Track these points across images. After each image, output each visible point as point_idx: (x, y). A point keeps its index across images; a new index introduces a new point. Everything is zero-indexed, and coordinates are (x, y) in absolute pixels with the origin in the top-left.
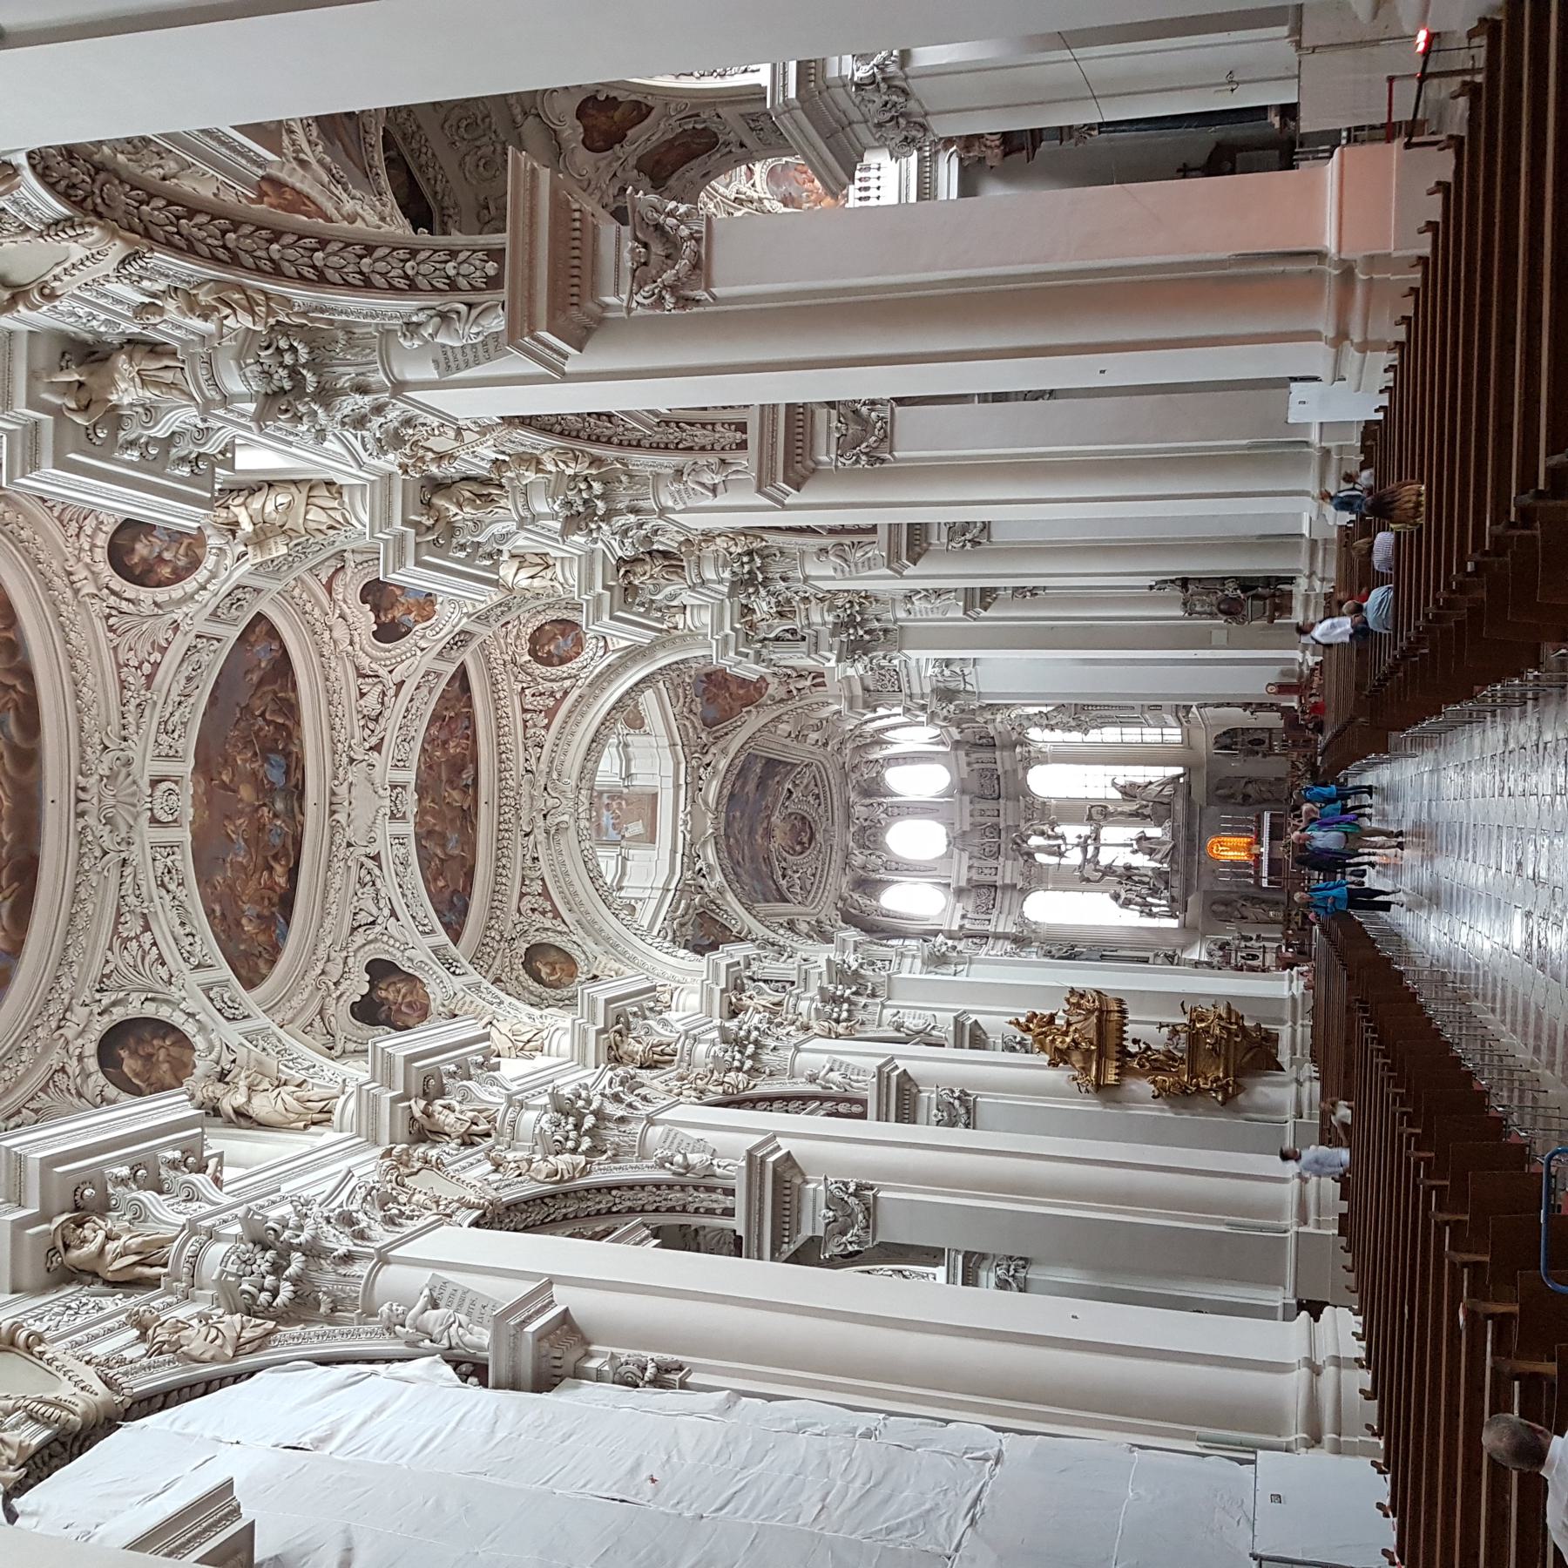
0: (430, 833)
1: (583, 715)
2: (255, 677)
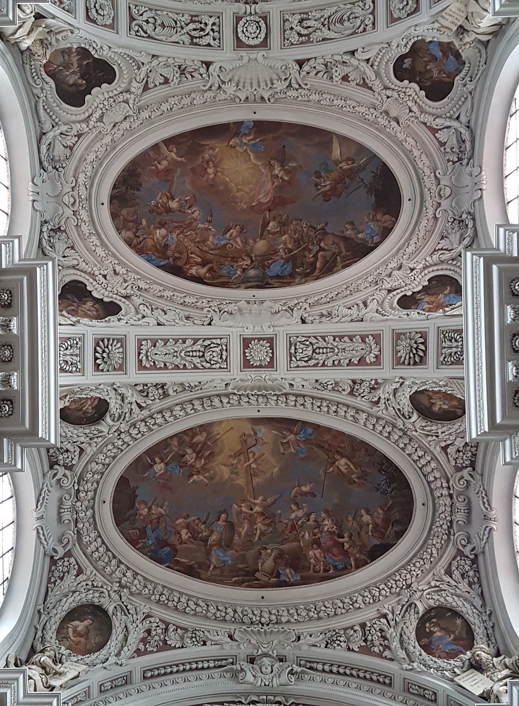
0: (231, 526)
1: (370, 691)
2: (349, 233)
